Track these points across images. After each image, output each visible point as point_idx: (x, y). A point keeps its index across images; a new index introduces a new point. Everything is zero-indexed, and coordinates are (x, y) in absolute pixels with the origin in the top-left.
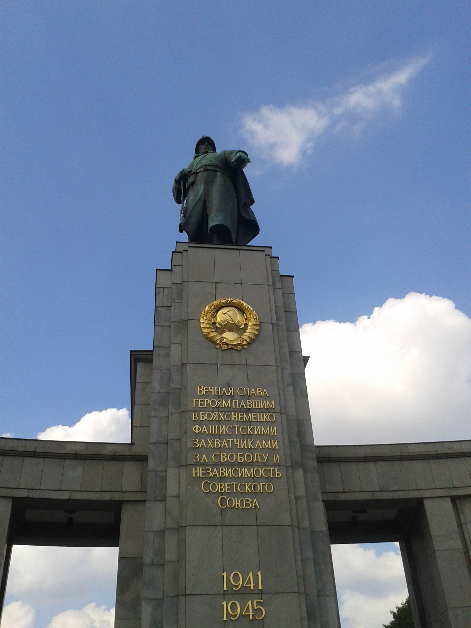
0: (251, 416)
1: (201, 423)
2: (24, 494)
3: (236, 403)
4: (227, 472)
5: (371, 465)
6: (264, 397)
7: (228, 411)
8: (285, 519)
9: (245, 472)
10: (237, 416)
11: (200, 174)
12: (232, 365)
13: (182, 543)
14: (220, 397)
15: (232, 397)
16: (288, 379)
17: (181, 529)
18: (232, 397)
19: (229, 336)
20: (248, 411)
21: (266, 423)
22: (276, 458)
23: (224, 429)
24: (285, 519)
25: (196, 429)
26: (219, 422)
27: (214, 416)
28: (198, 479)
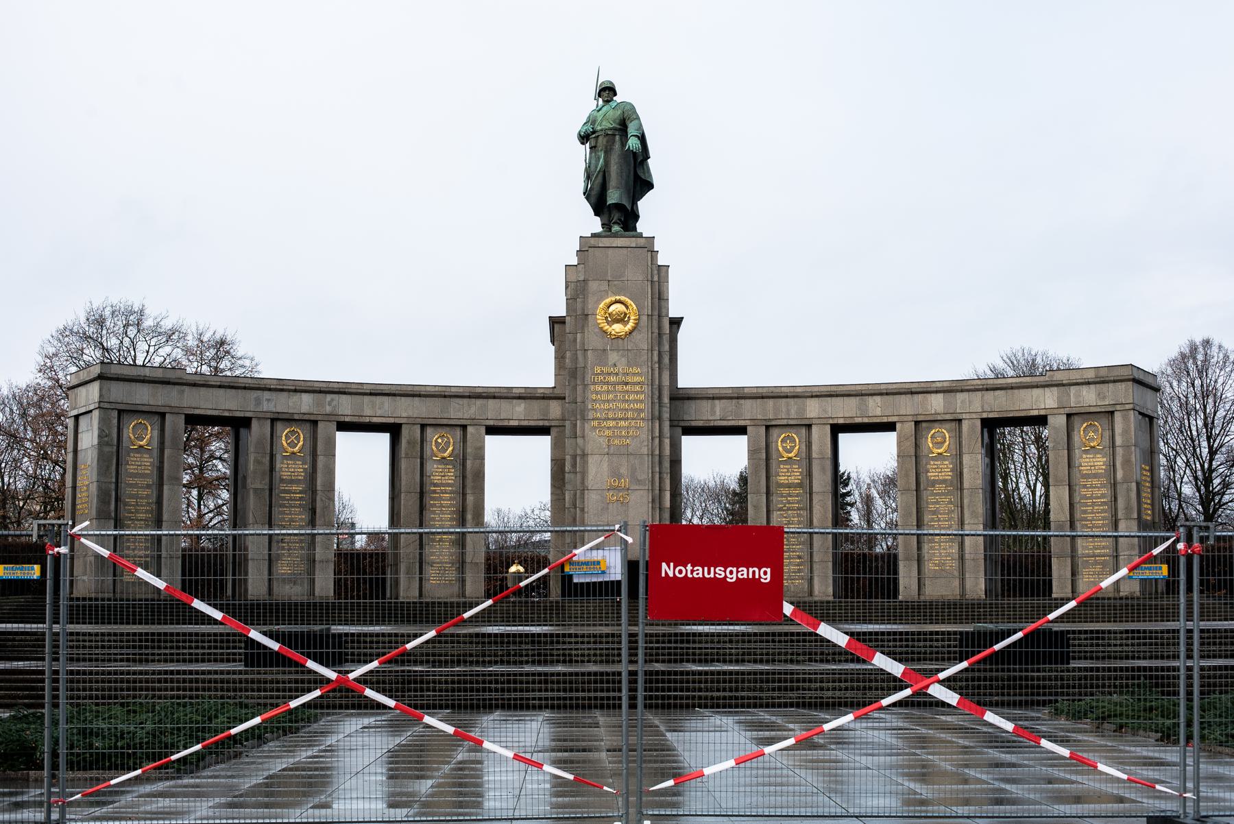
0: (629, 387)
1: (597, 393)
2: (491, 423)
3: (621, 378)
4: (612, 424)
5: (717, 402)
7: (614, 384)
8: (645, 451)
9: (622, 423)
10: (619, 388)
11: (600, 139)
12: (618, 350)
13: (585, 463)
14: (609, 374)
15: (617, 374)
16: (656, 358)
17: (584, 455)
18: (617, 374)
19: (618, 328)
20: (626, 384)
21: (637, 393)
22: (642, 415)
26: (608, 392)
27: (605, 387)
28: (594, 428)
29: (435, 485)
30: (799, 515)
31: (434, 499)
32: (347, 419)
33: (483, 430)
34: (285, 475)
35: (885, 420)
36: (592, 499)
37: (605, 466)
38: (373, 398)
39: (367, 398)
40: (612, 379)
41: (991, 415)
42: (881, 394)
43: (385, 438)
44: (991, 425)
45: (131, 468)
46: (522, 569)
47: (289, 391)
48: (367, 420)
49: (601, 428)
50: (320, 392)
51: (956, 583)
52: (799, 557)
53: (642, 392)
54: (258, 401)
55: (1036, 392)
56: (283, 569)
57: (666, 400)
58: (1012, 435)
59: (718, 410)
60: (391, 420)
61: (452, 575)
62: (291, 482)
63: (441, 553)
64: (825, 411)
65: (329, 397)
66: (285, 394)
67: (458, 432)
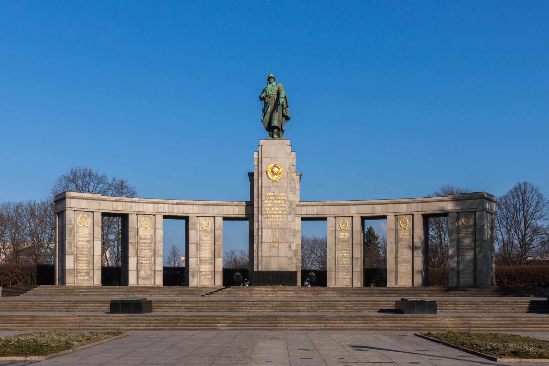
0: (279, 201)
1: (266, 204)
2: (225, 216)
6: (283, 196)
7: (273, 200)
9: (277, 216)
10: (276, 201)
15: (274, 196)
16: (290, 190)
18: (274, 196)
20: (278, 200)
21: (283, 204)
22: (285, 213)
23: (272, 205)
24: (285, 227)
25: (265, 205)
26: (271, 203)
27: (270, 201)
29: (203, 241)
30: (347, 253)
31: (202, 246)
32: (167, 214)
33: (221, 219)
34: (142, 237)
35: (382, 214)
36: (265, 246)
37: (270, 233)
38: (177, 206)
39: (175, 206)
40: (273, 198)
41: (426, 213)
42: (381, 204)
43: (184, 221)
44: (426, 217)
45: (81, 234)
46: (240, 274)
47: (144, 203)
48: (175, 215)
49: (268, 218)
50: (156, 203)
51: (410, 280)
52: (347, 270)
53: (284, 203)
54: (131, 207)
55: (444, 202)
56: (142, 274)
57: (294, 206)
58: (431, 219)
59: (315, 210)
60: (185, 215)
61: (210, 276)
62: (145, 239)
63: (206, 268)
64: (358, 211)
65: (160, 205)
66: (142, 204)
67: (212, 219)
